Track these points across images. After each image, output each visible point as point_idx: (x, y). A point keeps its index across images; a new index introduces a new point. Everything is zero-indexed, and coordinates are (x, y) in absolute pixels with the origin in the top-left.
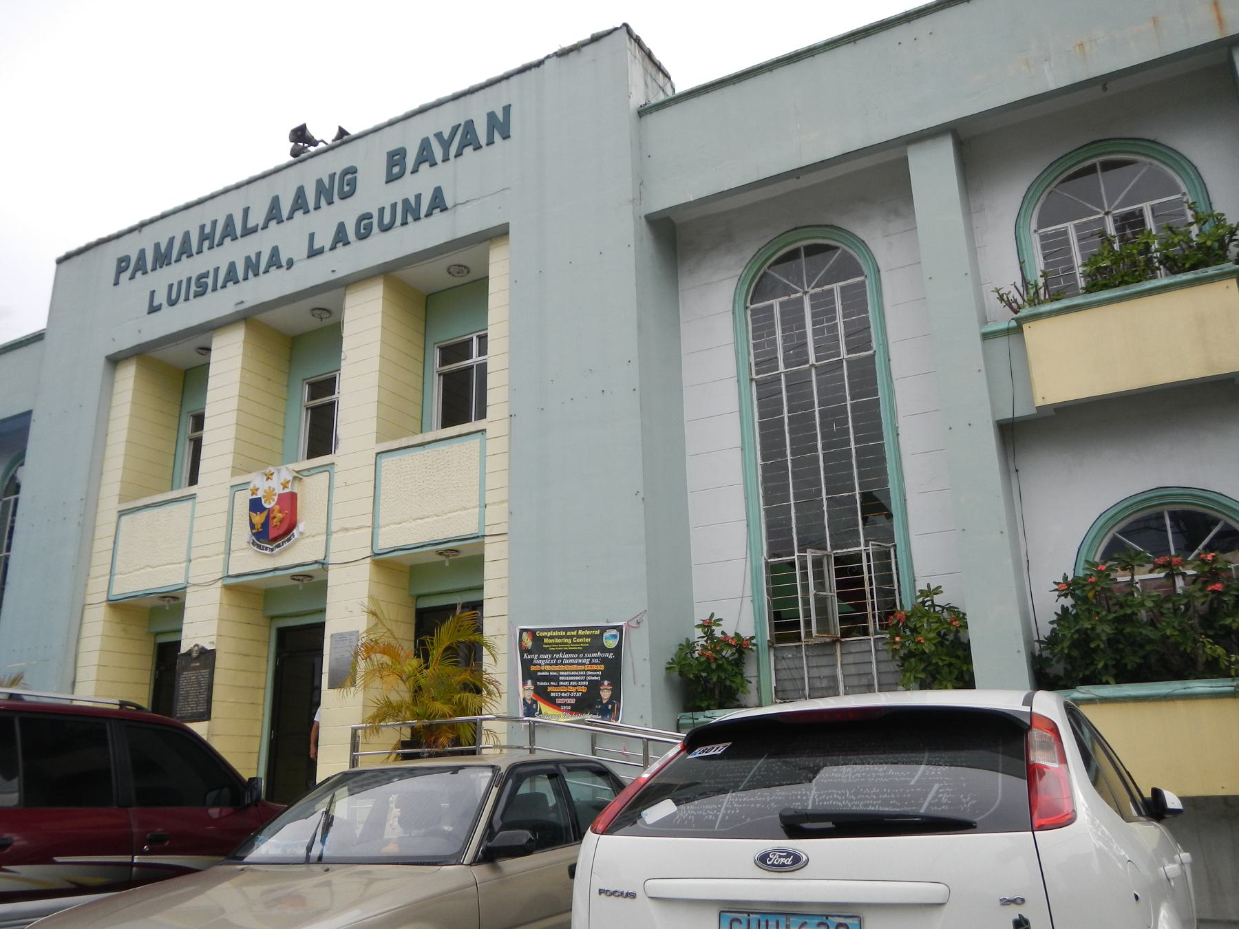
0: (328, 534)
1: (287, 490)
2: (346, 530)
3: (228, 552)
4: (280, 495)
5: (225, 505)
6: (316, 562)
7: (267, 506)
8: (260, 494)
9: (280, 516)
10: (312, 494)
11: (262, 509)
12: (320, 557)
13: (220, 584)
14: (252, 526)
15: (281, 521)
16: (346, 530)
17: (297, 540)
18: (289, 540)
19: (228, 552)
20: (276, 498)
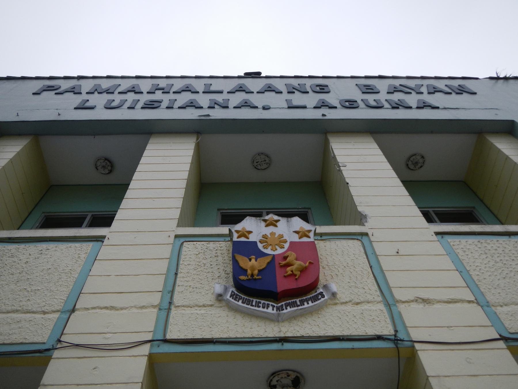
0: (390, 303)
1: (305, 239)
2: (426, 301)
3: (166, 307)
4: (291, 243)
5: (166, 252)
6: (379, 338)
7: (268, 251)
8: (252, 238)
9: (298, 264)
10: (339, 260)
11: (261, 254)
12: (387, 330)
13: (146, 349)
14: (238, 270)
15: (303, 270)
16: (426, 301)
17: (325, 305)
18: (315, 299)
19: (166, 307)
20: (287, 246)
